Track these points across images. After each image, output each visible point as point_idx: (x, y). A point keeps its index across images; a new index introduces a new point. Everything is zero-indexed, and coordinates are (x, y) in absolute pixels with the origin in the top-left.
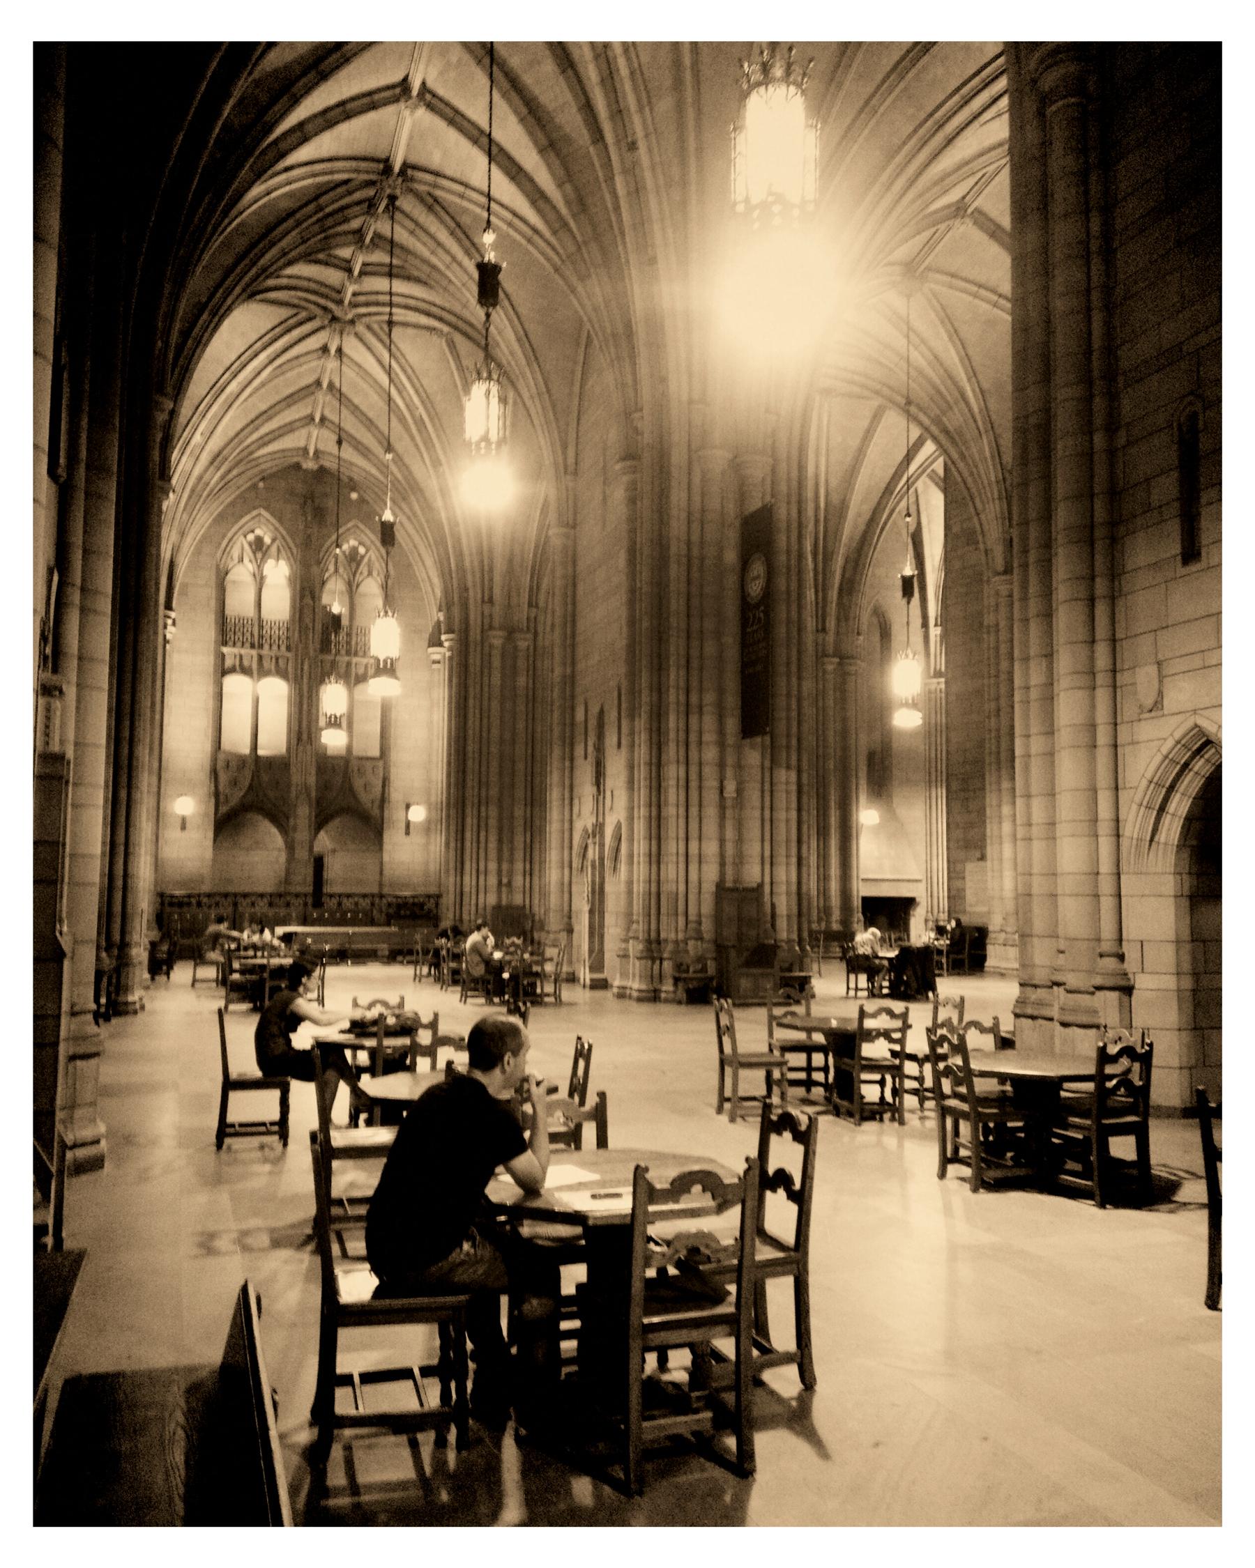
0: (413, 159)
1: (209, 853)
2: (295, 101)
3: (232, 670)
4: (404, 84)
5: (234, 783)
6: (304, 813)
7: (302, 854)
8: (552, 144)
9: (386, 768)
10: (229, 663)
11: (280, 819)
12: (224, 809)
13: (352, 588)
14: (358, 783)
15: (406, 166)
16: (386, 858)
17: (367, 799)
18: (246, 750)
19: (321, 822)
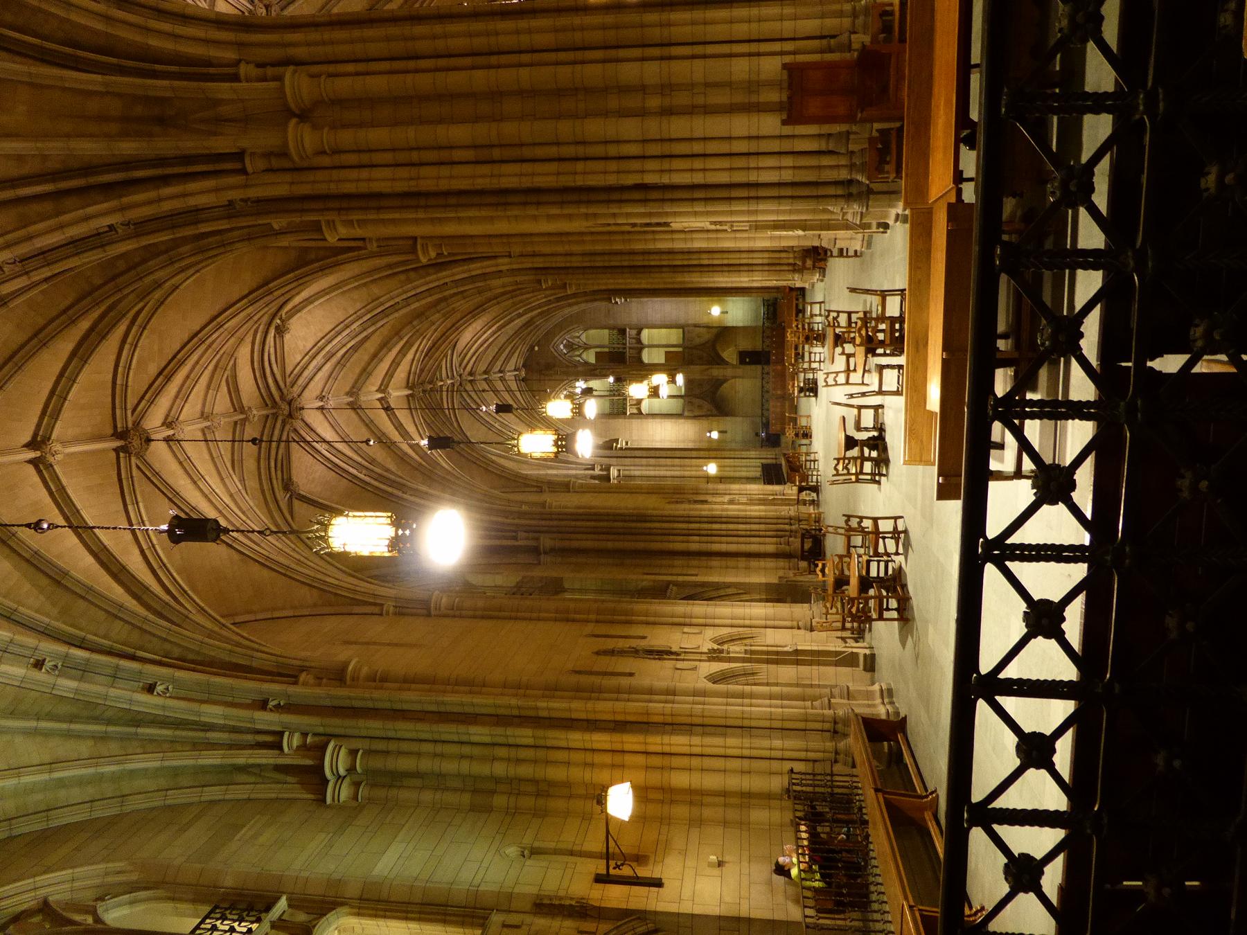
0: (404, 384)
1: (739, 419)
2: (406, 454)
3: (639, 409)
4: (380, 400)
5: (700, 407)
6: (717, 372)
7: (739, 371)
8: (397, 334)
9: (688, 325)
10: (635, 411)
11: (718, 383)
12: (715, 412)
13: (587, 347)
14: (698, 341)
15: (408, 387)
16: (741, 324)
17: (707, 336)
18: (681, 401)
19: (720, 361)
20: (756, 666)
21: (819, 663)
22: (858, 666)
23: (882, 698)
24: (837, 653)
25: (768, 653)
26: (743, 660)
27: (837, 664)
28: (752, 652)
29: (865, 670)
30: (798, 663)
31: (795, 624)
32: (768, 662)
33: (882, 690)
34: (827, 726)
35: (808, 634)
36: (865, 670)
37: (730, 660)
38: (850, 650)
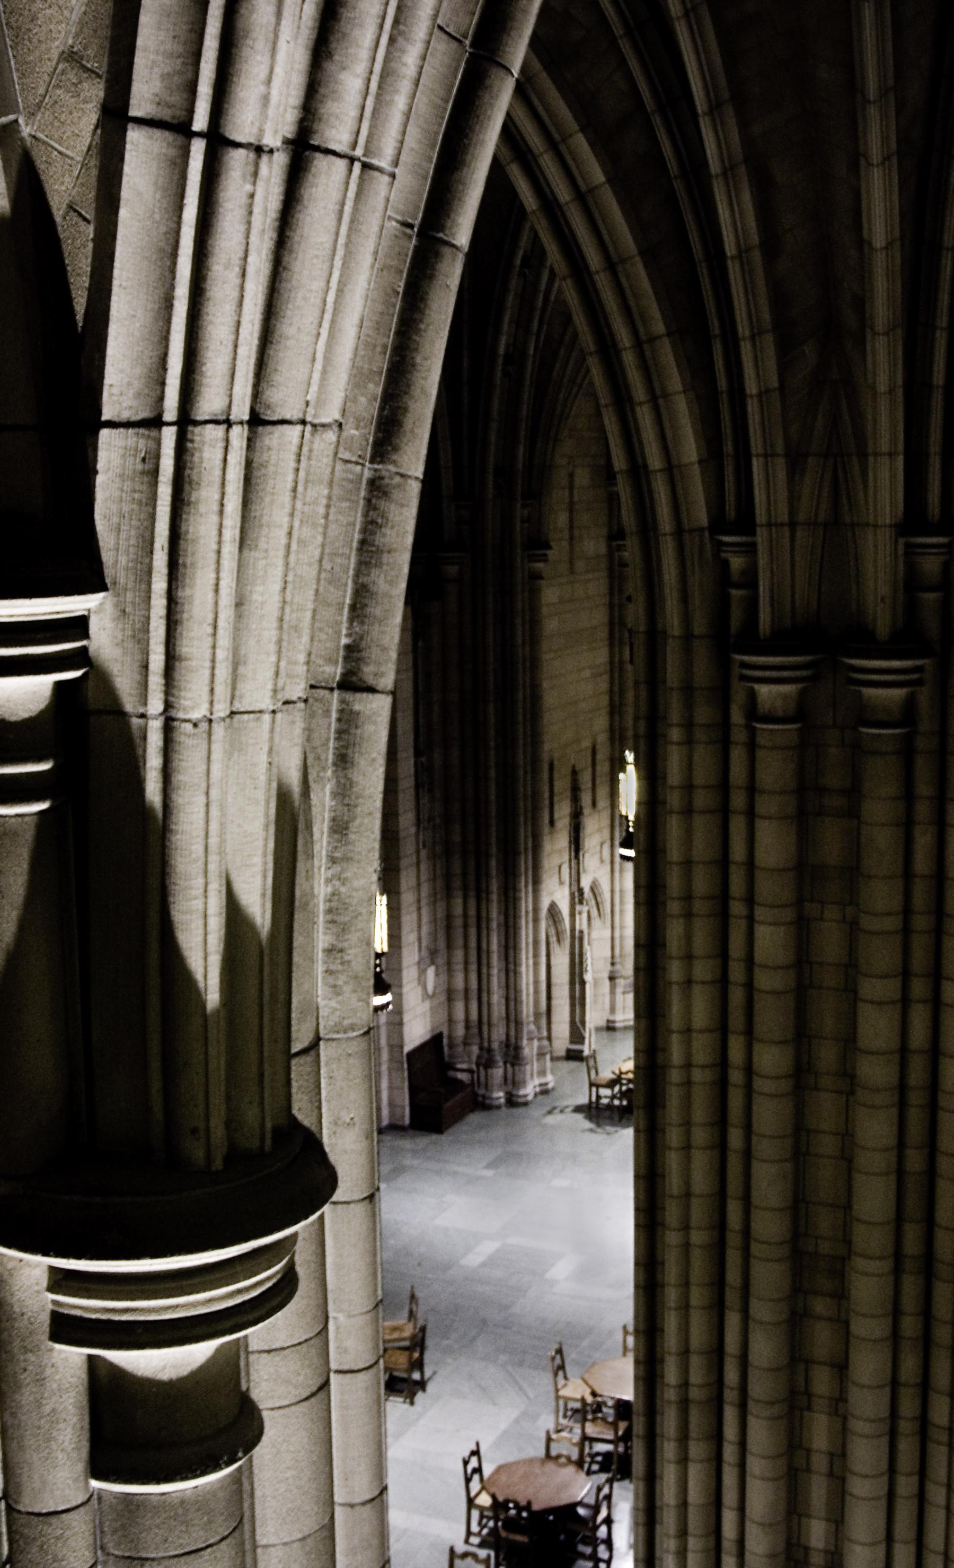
20: (567, 942)
21: (573, 1005)
22: (572, 1042)
23: (541, 1085)
24: (583, 1023)
25: (581, 955)
26: (573, 929)
27: (573, 1023)
28: (581, 939)
29: (568, 1051)
30: (572, 983)
31: (617, 960)
32: (572, 954)
33: (546, 1084)
34: (513, 1040)
35: (606, 975)
36: (568, 1051)
37: (572, 915)
38: (587, 1035)
